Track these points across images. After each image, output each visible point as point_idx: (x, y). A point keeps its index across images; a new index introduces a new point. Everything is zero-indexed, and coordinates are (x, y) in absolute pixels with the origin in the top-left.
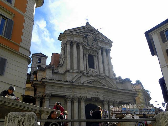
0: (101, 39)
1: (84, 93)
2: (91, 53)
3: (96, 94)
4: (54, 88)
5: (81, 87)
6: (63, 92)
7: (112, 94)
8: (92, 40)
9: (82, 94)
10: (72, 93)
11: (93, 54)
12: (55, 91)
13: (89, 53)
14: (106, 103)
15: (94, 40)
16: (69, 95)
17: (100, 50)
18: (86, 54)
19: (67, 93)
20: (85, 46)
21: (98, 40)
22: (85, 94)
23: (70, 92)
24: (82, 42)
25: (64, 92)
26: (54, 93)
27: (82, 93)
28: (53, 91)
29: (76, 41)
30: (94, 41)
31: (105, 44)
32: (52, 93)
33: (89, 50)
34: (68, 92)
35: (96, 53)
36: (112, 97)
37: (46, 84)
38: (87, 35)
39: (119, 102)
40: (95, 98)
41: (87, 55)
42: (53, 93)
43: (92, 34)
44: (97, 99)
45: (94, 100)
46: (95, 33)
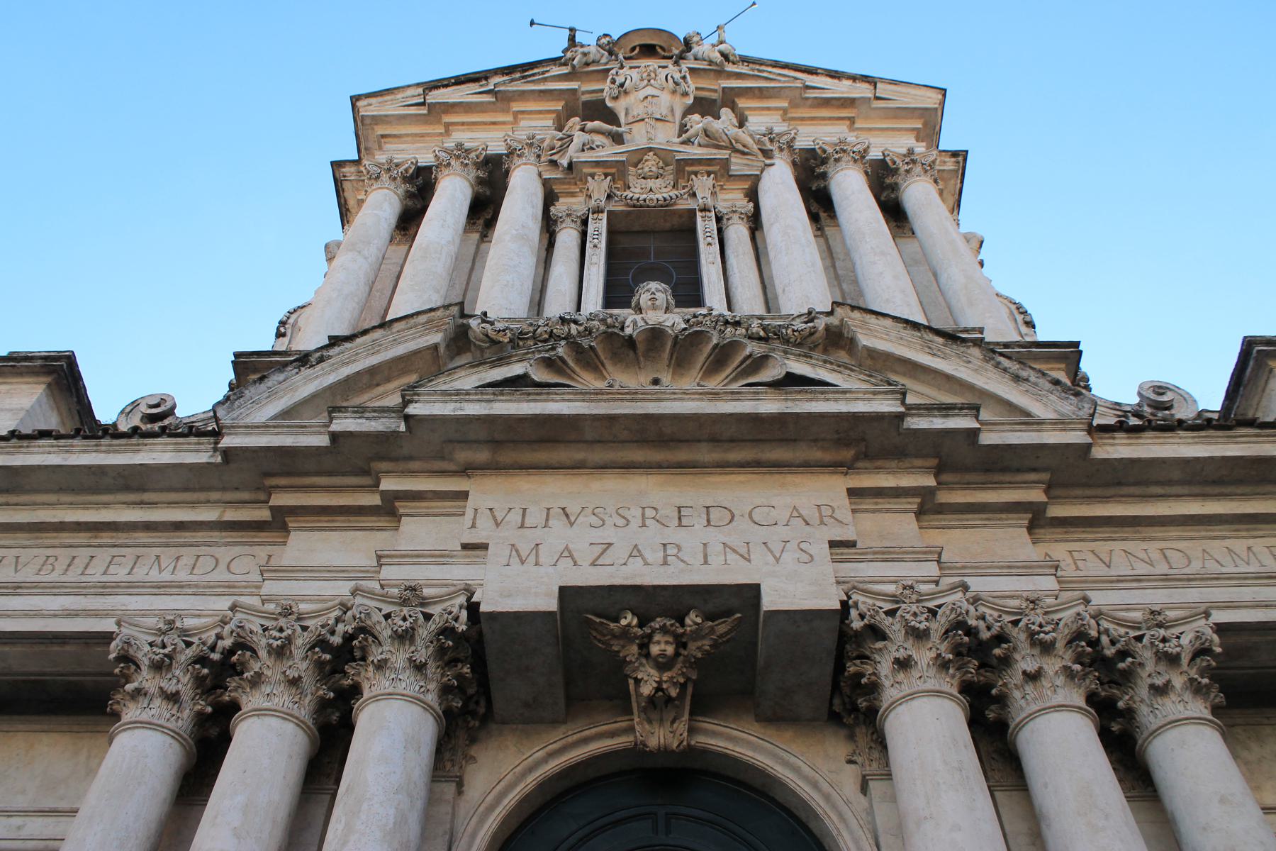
1: (440, 557)
3: (673, 534)
6: (79, 589)
15: (689, 111)
17: (767, 154)
18: (585, 222)
20: (563, 149)
21: (742, 103)
29: (468, 151)
31: (852, 120)
41: (599, 227)
45: (644, 646)
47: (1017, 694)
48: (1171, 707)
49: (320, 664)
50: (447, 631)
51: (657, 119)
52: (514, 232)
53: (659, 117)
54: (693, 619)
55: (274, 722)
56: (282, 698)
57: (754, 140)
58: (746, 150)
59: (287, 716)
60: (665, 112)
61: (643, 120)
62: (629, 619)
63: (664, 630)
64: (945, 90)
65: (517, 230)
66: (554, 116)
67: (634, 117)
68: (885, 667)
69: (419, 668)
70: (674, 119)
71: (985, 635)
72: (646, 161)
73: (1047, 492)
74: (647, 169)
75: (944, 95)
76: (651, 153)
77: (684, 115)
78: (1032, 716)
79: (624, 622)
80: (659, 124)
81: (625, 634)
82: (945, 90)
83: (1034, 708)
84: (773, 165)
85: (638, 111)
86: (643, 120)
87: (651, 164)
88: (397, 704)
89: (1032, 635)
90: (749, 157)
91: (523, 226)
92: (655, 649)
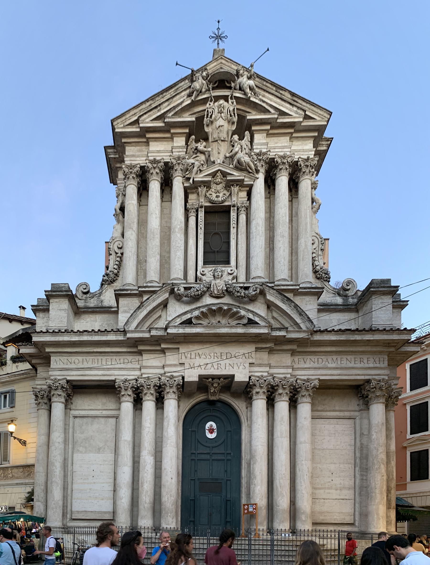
0: (267, 111)
2: (220, 199)
4: (77, 361)
5: (163, 346)
7: (292, 355)
8: (228, 133)
9: (167, 369)
10: (134, 369)
11: (226, 204)
12: (78, 369)
13: (211, 201)
14: (258, 390)
16: (123, 378)
17: (257, 171)
19: (116, 372)
20: (191, 172)
22: (179, 369)
23: (130, 366)
24: (179, 158)
25: (109, 369)
26: (74, 376)
27: (171, 365)
28: (71, 369)
30: (236, 137)
32: (69, 378)
33: (207, 185)
34: (120, 369)
35: (243, 194)
36: (287, 367)
37: (48, 350)
38: (200, 120)
39: (317, 383)
40: (219, 377)
42: (73, 376)
43: (225, 98)
44: (226, 381)
46: (240, 89)
47: (277, 396)
48: (304, 399)
49: (156, 390)
50: (178, 385)
51: (222, 141)
52: (179, 227)
53: (223, 139)
54: (222, 379)
55: (151, 402)
56: (151, 398)
57: (254, 164)
58: (251, 171)
59: (152, 401)
60: (225, 136)
61: (217, 141)
62: (210, 380)
63: (216, 382)
64: (330, 114)
65: (179, 225)
66: (185, 135)
67: (214, 138)
68: (254, 392)
69: (174, 392)
70: (228, 139)
71: (274, 385)
72: (218, 176)
73: (297, 346)
74: (217, 181)
75: (330, 116)
76: (219, 172)
77: (232, 137)
78: (278, 402)
79: (209, 380)
80: (223, 142)
81: (209, 382)
82: (330, 114)
83: (280, 400)
84: (258, 178)
85: (215, 136)
86: (217, 141)
87: (219, 180)
88: (172, 400)
89: (283, 385)
90: (251, 174)
91: (181, 222)
92: (214, 385)
